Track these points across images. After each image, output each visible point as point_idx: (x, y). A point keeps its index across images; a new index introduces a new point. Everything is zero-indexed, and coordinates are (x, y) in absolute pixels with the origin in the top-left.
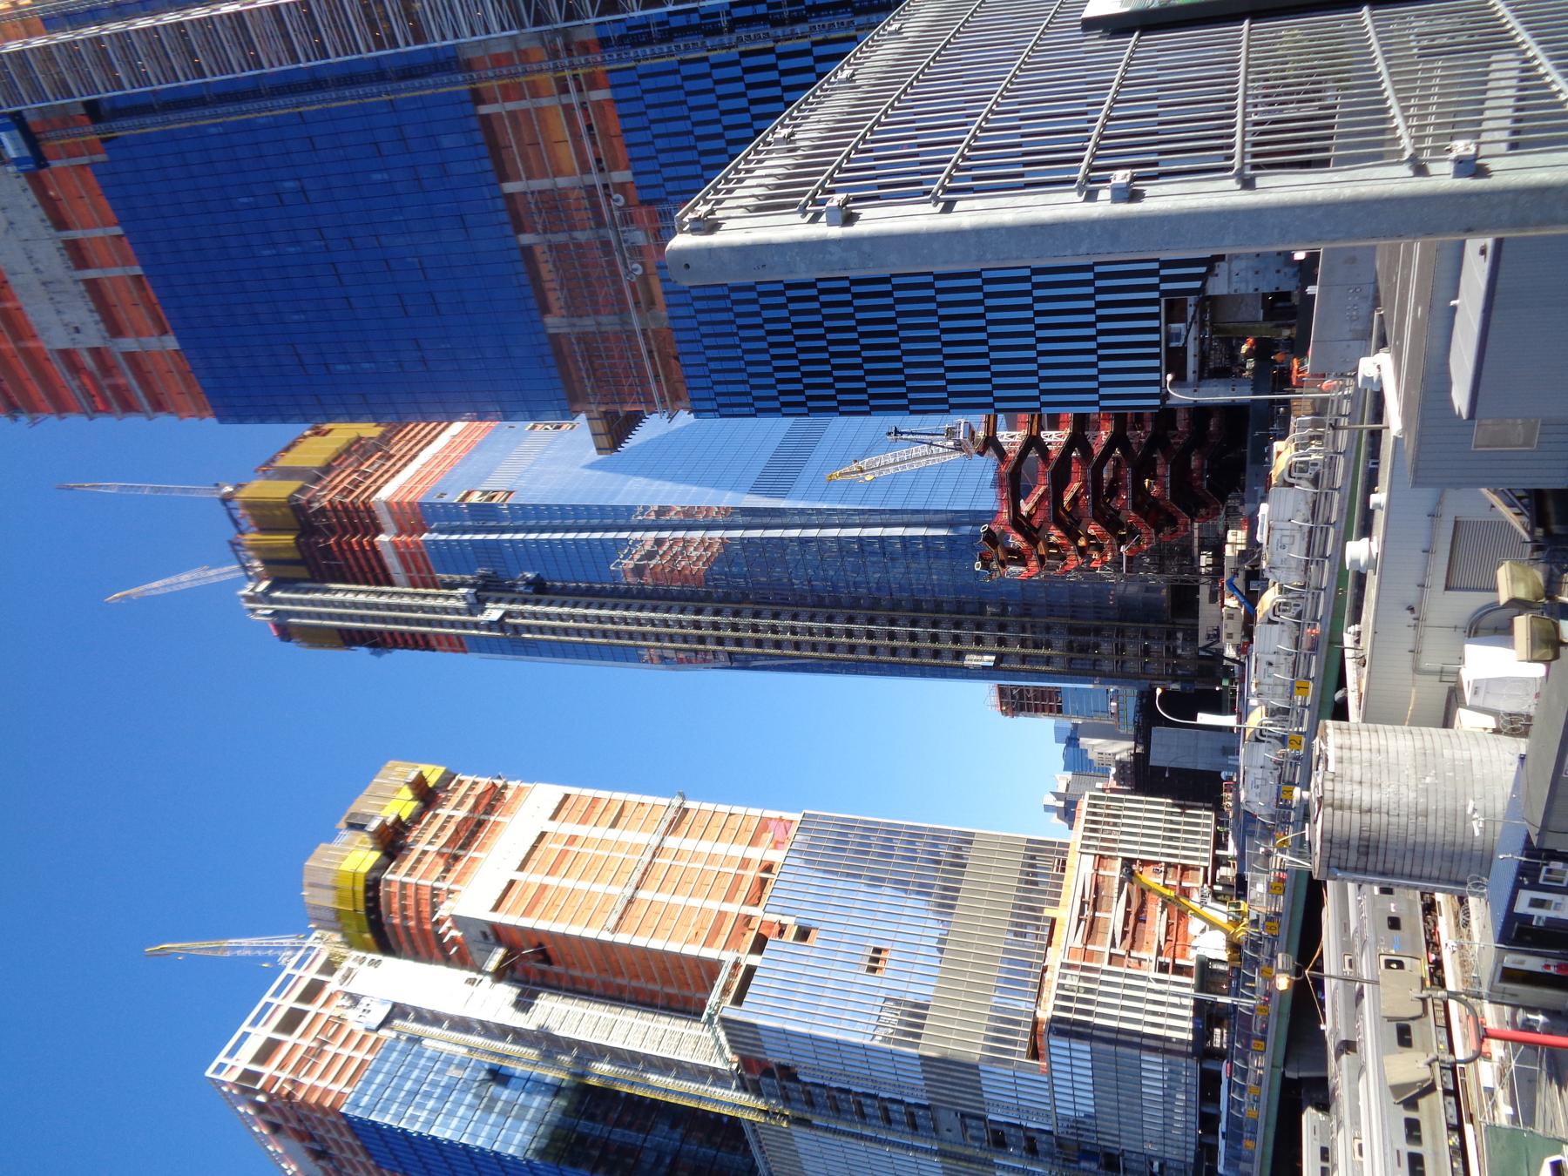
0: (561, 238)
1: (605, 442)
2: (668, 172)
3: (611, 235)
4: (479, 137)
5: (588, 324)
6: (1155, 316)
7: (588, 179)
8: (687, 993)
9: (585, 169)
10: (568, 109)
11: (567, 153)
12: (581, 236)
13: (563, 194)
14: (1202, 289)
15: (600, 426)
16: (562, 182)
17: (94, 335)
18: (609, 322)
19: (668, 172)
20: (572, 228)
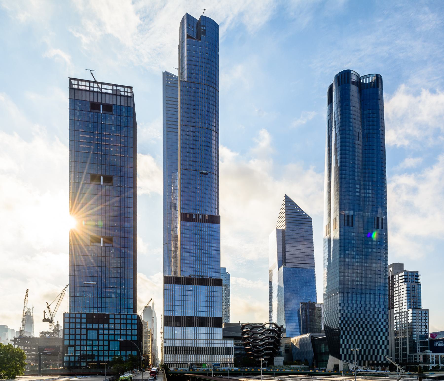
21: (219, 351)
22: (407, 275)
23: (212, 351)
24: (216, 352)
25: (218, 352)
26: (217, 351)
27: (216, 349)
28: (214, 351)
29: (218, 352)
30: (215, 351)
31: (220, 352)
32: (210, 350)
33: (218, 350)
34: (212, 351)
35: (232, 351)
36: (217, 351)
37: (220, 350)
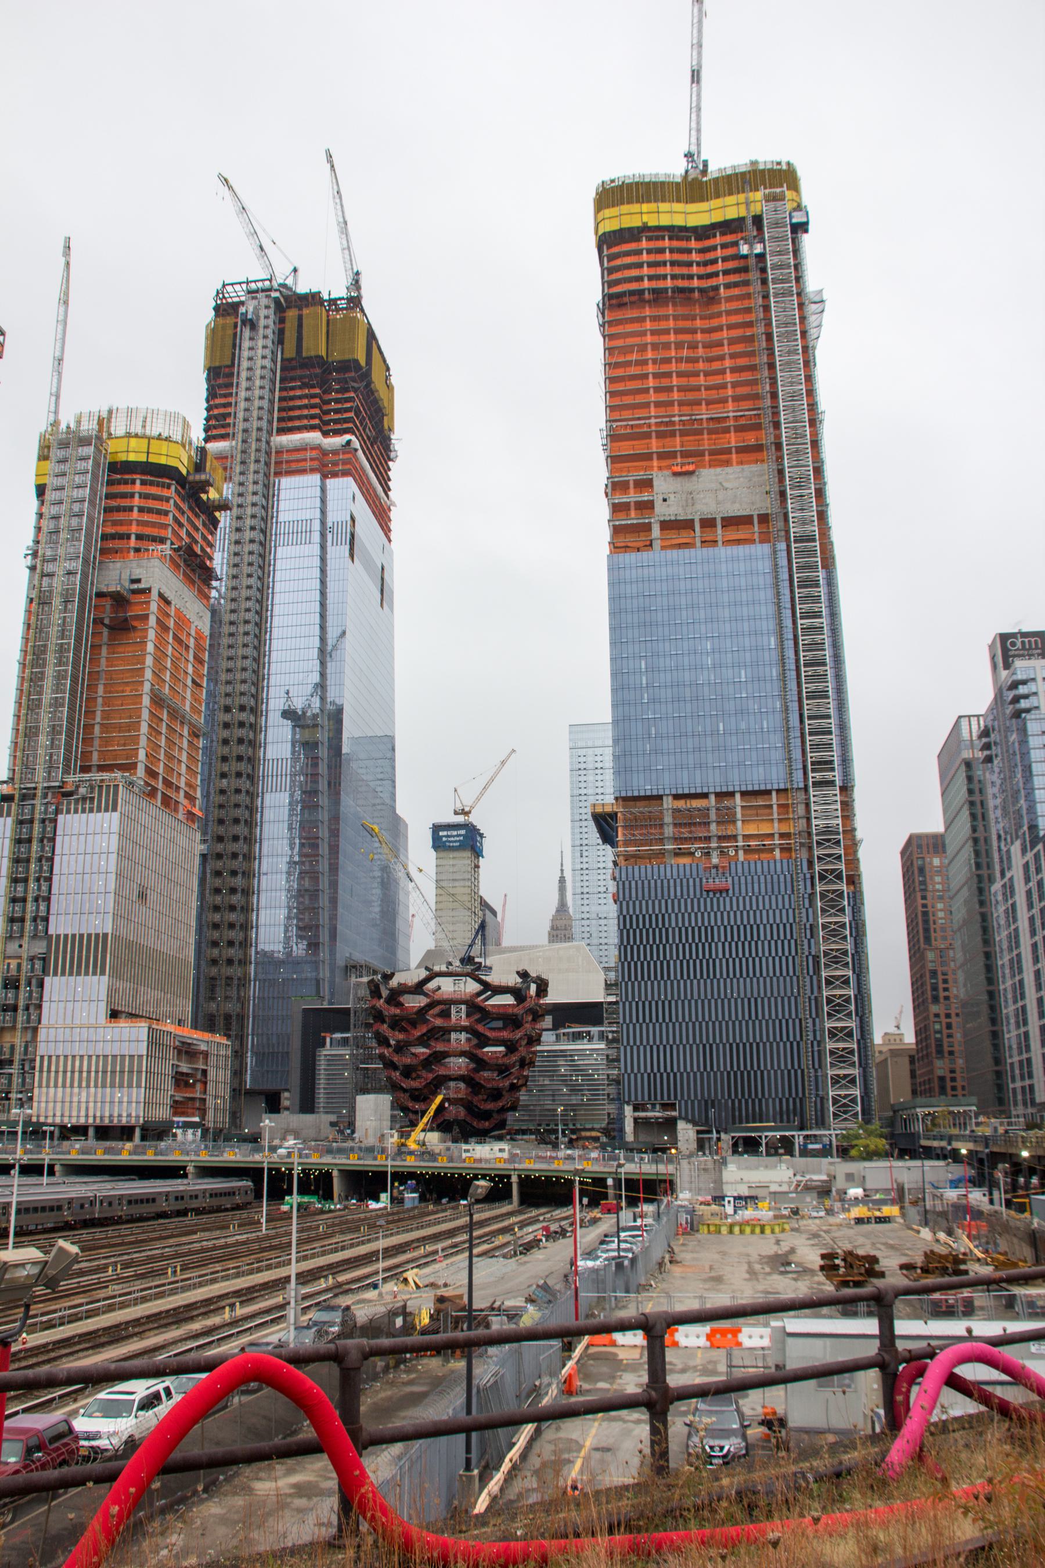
0: (713, 815)
1: (599, 810)
2: (743, 879)
3: (714, 845)
4: (763, 788)
5: (668, 819)
6: (662, 1098)
7: (740, 838)
8: (96, 742)
9: (746, 837)
10: (771, 836)
11: (752, 830)
12: (713, 827)
13: (734, 822)
14: (680, 1118)
15: (608, 809)
16: (739, 824)
17: (663, 511)
18: (669, 831)
19: (743, 879)
20: (718, 823)
21: (89, 1072)
22: (1033, 680)
23: (61, 1074)
24: (77, 1075)
25: (85, 1075)
26: (81, 1072)
27: (77, 1063)
28: (69, 1074)
29: (85, 1075)
30: (73, 1072)
31: (93, 1074)
32: (53, 1068)
33: (85, 1068)
34: (61, 1074)
35: (140, 1072)
36: (81, 1072)
37: (93, 1069)
